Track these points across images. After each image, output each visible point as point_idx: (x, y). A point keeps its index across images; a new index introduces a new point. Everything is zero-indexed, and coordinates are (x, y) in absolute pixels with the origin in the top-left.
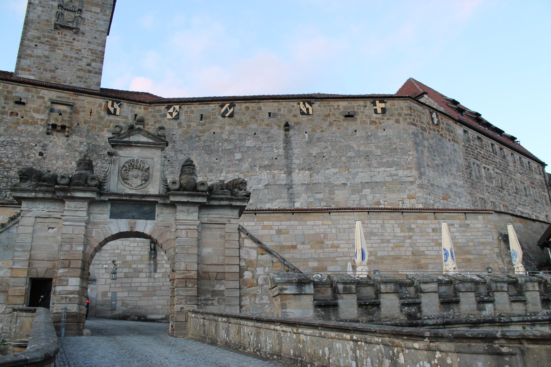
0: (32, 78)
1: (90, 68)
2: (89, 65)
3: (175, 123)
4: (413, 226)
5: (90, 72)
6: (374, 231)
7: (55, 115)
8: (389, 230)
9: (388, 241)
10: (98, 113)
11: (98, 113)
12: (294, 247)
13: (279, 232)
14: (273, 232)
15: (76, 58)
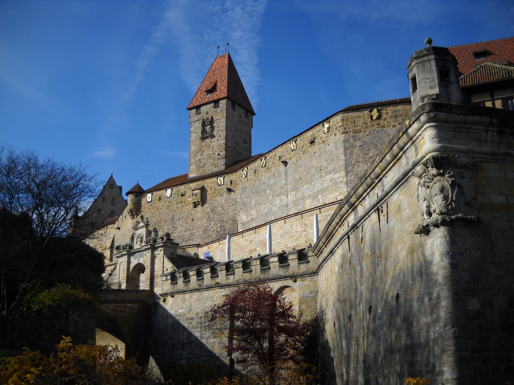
0: (195, 175)
1: (219, 157)
2: (219, 155)
3: (246, 179)
4: (307, 222)
5: (219, 159)
6: (287, 231)
7: (194, 196)
8: (295, 228)
9: (294, 236)
10: (214, 187)
11: (214, 187)
12: (255, 250)
13: (251, 242)
14: (248, 243)
15: (213, 154)
